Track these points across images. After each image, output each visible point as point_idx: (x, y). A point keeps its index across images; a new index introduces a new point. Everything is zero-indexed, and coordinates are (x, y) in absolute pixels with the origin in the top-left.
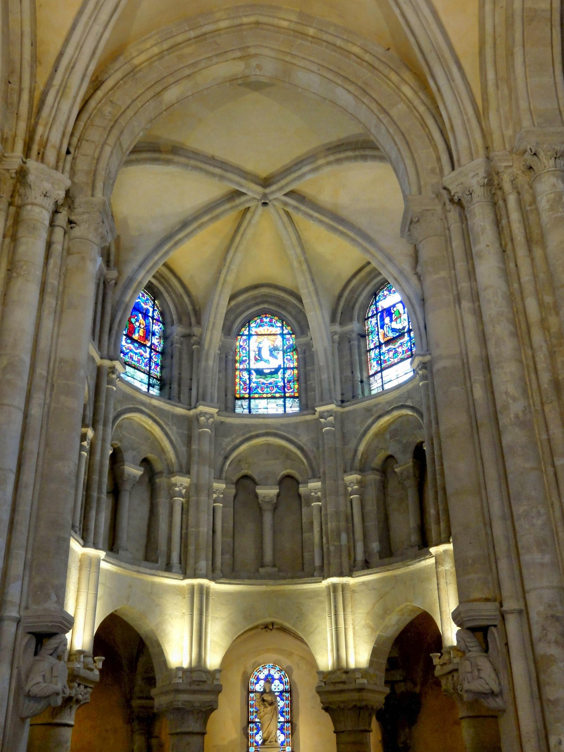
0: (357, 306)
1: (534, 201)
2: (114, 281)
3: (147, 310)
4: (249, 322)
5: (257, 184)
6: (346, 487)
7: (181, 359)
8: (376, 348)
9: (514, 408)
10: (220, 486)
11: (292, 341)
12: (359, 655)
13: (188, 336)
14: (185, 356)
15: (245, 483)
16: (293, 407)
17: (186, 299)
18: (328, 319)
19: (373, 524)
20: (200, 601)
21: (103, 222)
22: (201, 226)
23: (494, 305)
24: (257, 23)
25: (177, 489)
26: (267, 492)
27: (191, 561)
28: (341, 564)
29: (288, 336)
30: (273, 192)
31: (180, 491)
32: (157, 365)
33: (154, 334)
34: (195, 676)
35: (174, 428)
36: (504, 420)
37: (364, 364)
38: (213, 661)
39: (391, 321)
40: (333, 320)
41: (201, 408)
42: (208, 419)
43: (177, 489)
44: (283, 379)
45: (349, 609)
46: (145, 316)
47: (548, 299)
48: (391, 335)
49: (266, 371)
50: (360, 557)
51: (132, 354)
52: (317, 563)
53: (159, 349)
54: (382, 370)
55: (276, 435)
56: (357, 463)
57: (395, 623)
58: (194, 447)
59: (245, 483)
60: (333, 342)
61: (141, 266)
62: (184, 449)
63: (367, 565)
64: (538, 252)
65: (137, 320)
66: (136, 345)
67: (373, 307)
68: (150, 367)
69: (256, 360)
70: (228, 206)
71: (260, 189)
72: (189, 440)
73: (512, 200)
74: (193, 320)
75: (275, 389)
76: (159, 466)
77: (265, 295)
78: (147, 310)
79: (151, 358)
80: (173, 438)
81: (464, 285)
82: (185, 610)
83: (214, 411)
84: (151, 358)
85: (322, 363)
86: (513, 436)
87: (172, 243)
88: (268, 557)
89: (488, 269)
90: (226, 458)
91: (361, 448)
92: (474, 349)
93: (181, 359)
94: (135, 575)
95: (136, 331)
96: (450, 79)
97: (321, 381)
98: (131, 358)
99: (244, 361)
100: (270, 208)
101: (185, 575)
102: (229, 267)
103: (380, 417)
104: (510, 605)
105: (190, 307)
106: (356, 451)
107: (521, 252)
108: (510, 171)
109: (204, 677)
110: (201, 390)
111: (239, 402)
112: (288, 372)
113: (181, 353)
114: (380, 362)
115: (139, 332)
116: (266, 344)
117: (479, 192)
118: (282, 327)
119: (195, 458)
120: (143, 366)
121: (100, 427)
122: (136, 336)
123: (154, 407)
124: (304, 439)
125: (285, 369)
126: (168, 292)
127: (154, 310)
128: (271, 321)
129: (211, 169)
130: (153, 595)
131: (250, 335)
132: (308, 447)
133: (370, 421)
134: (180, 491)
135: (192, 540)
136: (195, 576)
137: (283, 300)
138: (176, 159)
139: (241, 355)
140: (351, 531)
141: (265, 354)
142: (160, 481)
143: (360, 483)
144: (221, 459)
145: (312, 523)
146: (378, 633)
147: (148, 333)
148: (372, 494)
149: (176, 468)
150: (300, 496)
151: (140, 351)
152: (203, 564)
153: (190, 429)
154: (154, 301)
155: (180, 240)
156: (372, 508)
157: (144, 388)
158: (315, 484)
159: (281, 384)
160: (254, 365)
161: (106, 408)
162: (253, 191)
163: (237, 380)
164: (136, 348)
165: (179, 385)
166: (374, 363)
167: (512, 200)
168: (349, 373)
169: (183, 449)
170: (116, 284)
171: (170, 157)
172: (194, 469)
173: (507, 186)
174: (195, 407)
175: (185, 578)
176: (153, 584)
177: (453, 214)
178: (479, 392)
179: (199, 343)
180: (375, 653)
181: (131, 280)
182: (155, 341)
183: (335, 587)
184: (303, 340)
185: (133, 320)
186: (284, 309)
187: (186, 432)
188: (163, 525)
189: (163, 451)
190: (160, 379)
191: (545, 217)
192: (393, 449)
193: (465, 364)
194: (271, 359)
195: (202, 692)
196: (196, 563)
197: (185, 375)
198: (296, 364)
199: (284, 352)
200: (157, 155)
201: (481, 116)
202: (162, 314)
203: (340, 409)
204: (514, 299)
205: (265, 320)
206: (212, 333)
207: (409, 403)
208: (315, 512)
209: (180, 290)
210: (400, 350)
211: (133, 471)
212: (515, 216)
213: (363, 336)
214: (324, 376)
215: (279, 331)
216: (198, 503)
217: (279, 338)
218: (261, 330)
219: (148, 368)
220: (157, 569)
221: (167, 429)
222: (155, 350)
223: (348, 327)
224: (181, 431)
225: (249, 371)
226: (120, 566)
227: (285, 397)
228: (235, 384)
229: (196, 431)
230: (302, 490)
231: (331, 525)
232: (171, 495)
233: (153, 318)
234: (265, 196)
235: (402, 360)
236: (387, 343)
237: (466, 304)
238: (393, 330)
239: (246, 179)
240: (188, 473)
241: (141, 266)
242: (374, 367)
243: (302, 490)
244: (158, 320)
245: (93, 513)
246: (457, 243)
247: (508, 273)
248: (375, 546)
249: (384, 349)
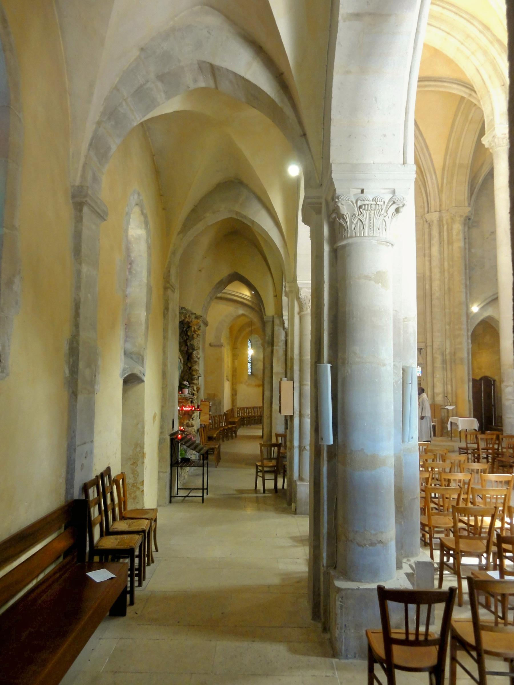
1: (452, 229)
9: (437, 293)
23: (435, 262)
36: (433, 297)
47: (451, 263)
64: (450, 247)
73: (445, 227)
81: (427, 252)
86: (435, 302)
89: (435, 250)
92: (428, 274)
96: (432, 179)
104: (429, 344)
107: (446, 247)
108: (446, 216)
117: (435, 222)
167: (445, 227)
173: (444, 222)
177: (426, 226)
178: (427, 287)
191: (454, 237)
201: (440, 191)
204: (442, 261)
212: (445, 233)
237: (427, 258)
246: (426, 237)
247: (441, 252)
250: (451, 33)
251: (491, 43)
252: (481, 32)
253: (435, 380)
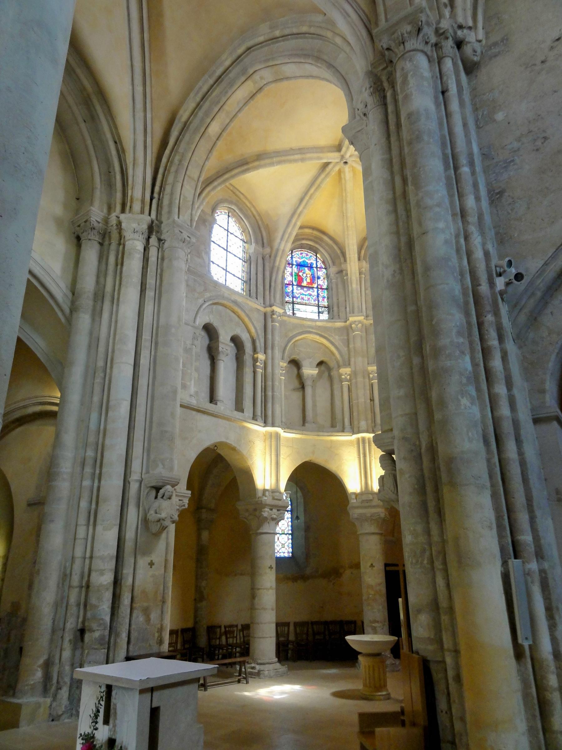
2: (268, 256)
3: (312, 264)
5: (332, 152)
7: (337, 289)
13: (341, 272)
14: (340, 286)
17: (335, 247)
21: (182, 232)
22: (311, 198)
24: (249, 49)
25: (343, 377)
27: (356, 423)
30: (346, 153)
31: (346, 377)
32: (324, 298)
33: (319, 278)
34: (364, 497)
35: (337, 337)
41: (351, 319)
42: (357, 325)
43: (343, 377)
46: (311, 267)
51: (303, 296)
53: (325, 287)
58: (351, 346)
61: (282, 239)
62: (346, 349)
65: (304, 273)
66: (305, 289)
68: (318, 301)
70: (323, 176)
71: (337, 154)
72: (347, 343)
74: (342, 259)
76: (332, 364)
78: (312, 264)
79: (318, 294)
80: (337, 344)
82: (355, 454)
83: (361, 318)
84: (318, 294)
87: (296, 216)
93: (337, 289)
94: (316, 438)
95: (304, 280)
98: (303, 299)
101: (354, 433)
102: (347, 216)
105: (339, 252)
109: (371, 497)
113: (337, 285)
115: (306, 280)
119: (352, 354)
120: (313, 302)
121: (269, 351)
122: (304, 284)
123: (319, 327)
126: (322, 247)
127: (317, 262)
129: (292, 157)
130: (332, 449)
134: (346, 377)
135: (355, 409)
136: (359, 432)
138: (262, 162)
142: (334, 373)
147: (313, 279)
149: (341, 363)
151: (308, 292)
152: (363, 424)
153: (348, 335)
154: (316, 256)
155: (301, 212)
157: (315, 316)
161: (272, 338)
162: (333, 157)
164: (306, 291)
165: (338, 307)
169: (344, 350)
170: (270, 256)
171: (256, 163)
175: (353, 434)
176: (332, 441)
179: (347, 275)
181: (278, 250)
182: (320, 282)
185: (301, 274)
187: (346, 338)
188: (338, 403)
189: (332, 352)
190: (328, 307)
197: (342, 299)
200: (245, 167)
202: (323, 262)
206: (350, 266)
209: (330, 242)
211: (310, 371)
216: (356, 383)
219: (317, 302)
220: (338, 432)
221: (331, 339)
222: (321, 289)
224: (342, 338)
226: (302, 434)
229: (352, 335)
232: (341, 381)
233: (317, 267)
234: (342, 157)
239: (322, 152)
240: (348, 364)
241: (282, 239)
244: (321, 268)
245: (269, 405)
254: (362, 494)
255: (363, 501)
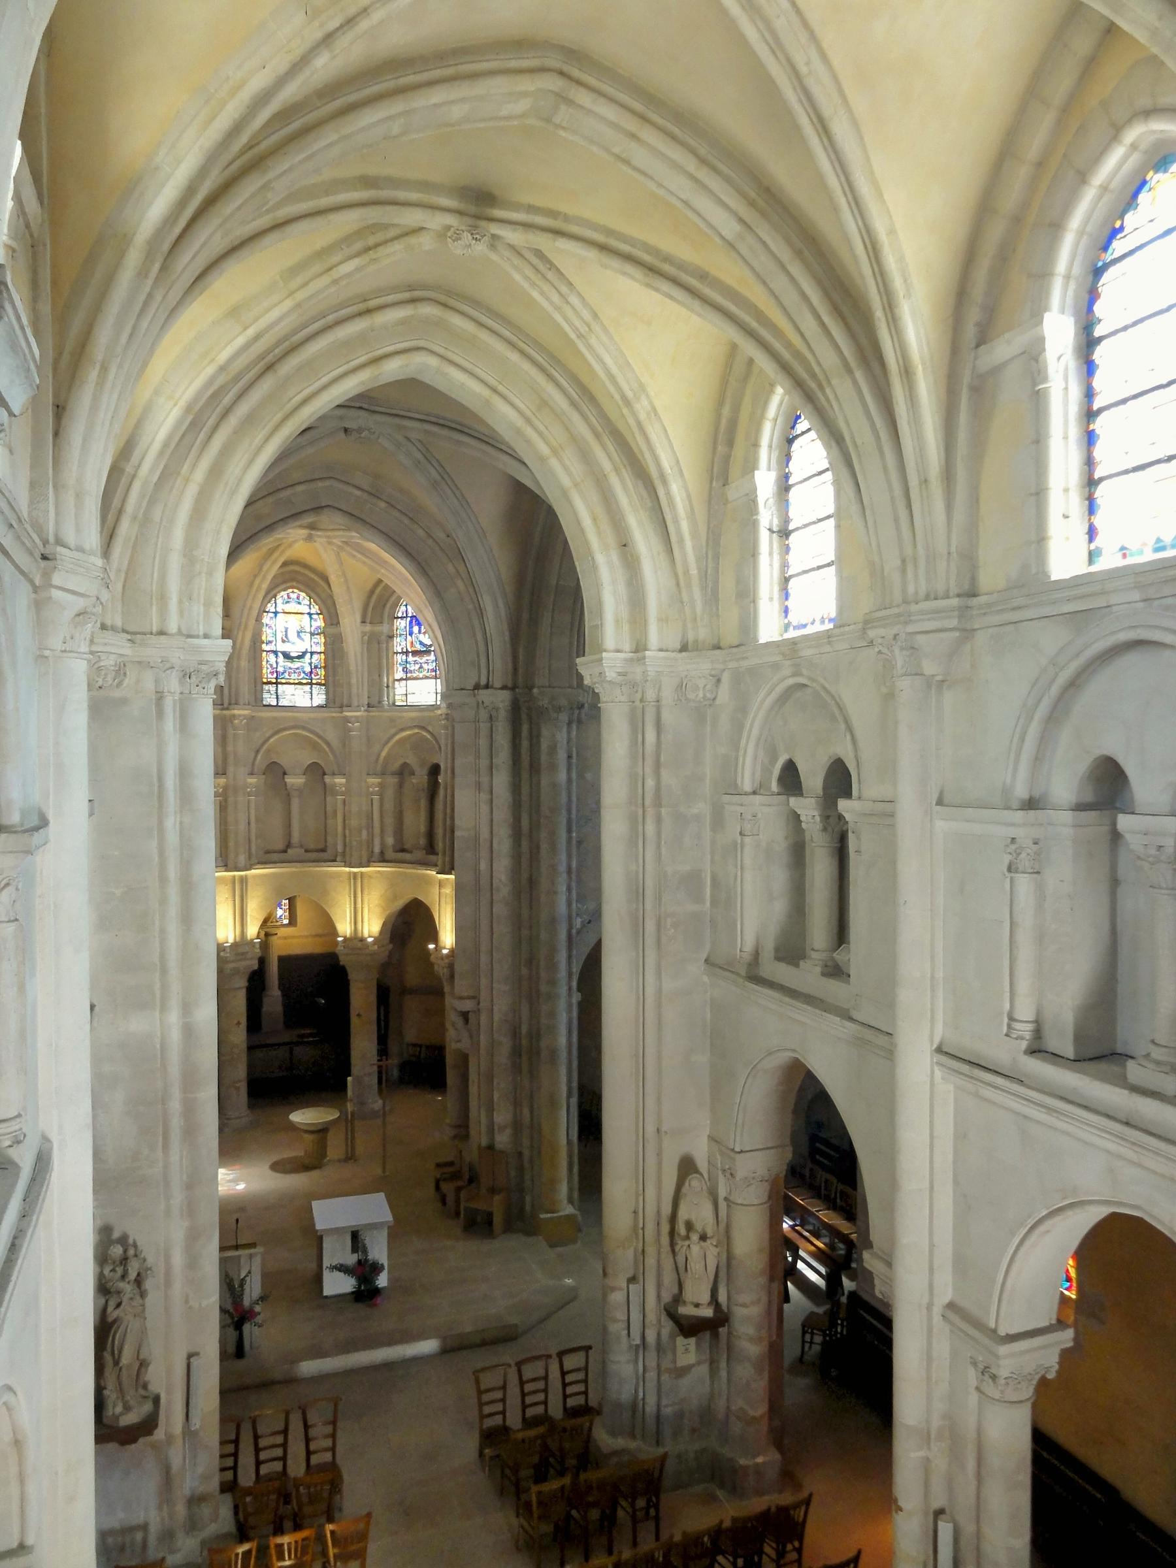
0: (388, 605)
4: (275, 596)
6: (368, 787)
8: (403, 653)
10: (252, 780)
11: (319, 622)
12: (372, 927)
15: (275, 772)
16: (319, 698)
18: (358, 618)
19: (390, 821)
20: (241, 890)
26: (295, 781)
27: (232, 856)
28: (361, 857)
29: (314, 616)
30: (319, 536)
34: (241, 950)
37: (390, 668)
38: (252, 930)
39: (420, 632)
40: (363, 622)
41: (236, 712)
44: (310, 664)
45: (366, 892)
48: (418, 647)
49: (293, 654)
50: (377, 850)
52: (340, 849)
54: (406, 679)
55: (304, 728)
56: (379, 768)
57: (400, 903)
58: (230, 748)
59: (275, 772)
60: (363, 643)
63: (383, 859)
67: (403, 608)
69: (283, 641)
75: (303, 675)
77: (296, 572)
81: (485, 779)
83: (246, 712)
85: (353, 668)
88: (296, 838)
90: (258, 751)
91: (384, 754)
92: (485, 833)
97: (349, 684)
99: (270, 642)
100: (317, 545)
103: (402, 730)
106: (379, 755)
109: (247, 949)
110: (233, 690)
111: (266, 687)
112: (315, 657)
114: (405, 670)
116: (294, 623)
118: (310, 606)
119: (231, 759)
124: (332, 735)
125: (312, 653)
128: (298, 598)
131: (276, 613)
132: (335, 743)
133: (393, 731)
135: (232, 837)
137: (313, 580)
139: (267, 634)
140: (370, 827)
141: (292, 635)
143: (381, 785)
144: (253, 754)
145: (335, 812)
146: (387, 913)
148: (390, 794)
150: (325, 784)
152: (242, 859)
156: (389, 805)
158: (340, 780)
159: (308, 669)
160: (281, 647)
163: (264, 663)
166: (400, 669)
168: (376, 677)
172: (231, 770)
174: (227, 709)
180: (384, 924)
183: (355, 874)
184: (332, 630)
186: (313, 590)
192: (412, 760)
193: (477, 838)
194: (297, 640)
195: (245, 959)
196: (237, 856)
198: (322, 649)
199: (312, 634)
203: (365, 714)
205: (292, 595)
207: (430, 728)
208: (340, 806)
210: (425, 666)
213: (391, 637)
214: (354, 681)
215: (306, 610)
217: (307, 617)
218: (288, 608)
223: (378, 628)
225: (275, 653)
227: (311, 684)
228: (261, 668)
229: (231, 732)
230: (327, 779)
231: (354, 822)
235: (427, 678)
236: (415, 653)
237: (484, 796)
238: (421, 643)
242: (399, 674)
243: (327, 779)
248: (390, 841)
249: (411, 658)
250: (500, 388)
251: (597, 436)
252: (573, 404)
253: (496, 1096)
254: (235, 945)
255: (237, 954)
